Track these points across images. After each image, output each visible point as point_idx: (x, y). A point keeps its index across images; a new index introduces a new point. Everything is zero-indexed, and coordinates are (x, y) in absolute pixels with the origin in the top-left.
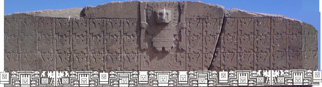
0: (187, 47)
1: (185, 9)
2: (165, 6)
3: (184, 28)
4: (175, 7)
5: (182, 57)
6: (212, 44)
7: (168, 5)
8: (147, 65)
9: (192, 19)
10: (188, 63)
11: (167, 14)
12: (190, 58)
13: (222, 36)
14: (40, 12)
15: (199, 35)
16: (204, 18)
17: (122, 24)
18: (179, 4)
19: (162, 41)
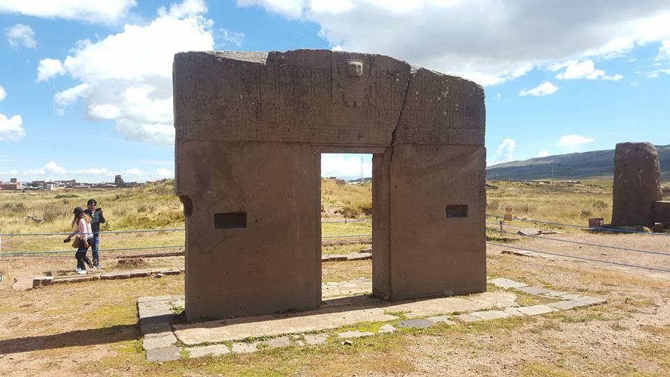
7: (360, 57)
11: (359, 66)
13: (408, 95)
14: (222, 53)
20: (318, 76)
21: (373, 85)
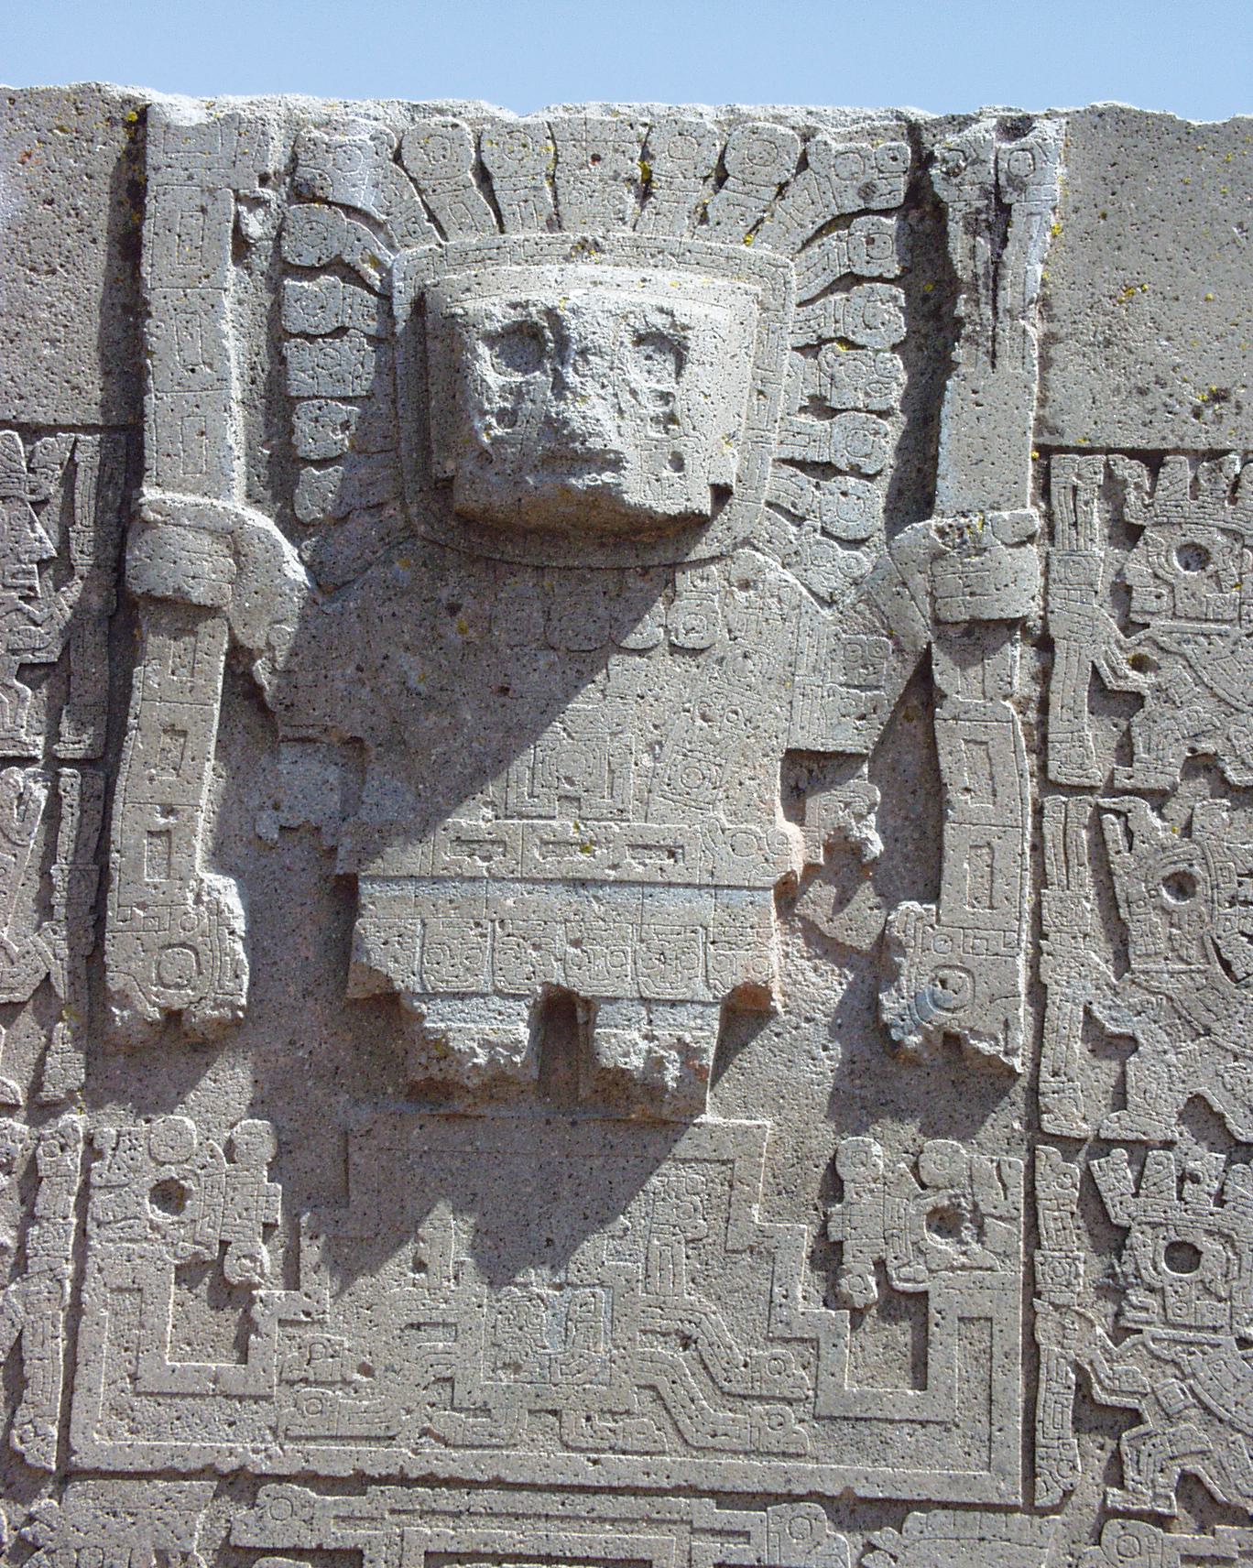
0: (1065, 1015)
2: (645, 191)
3: (1012, 624)
4: (842, 220)
5: (944, 1222)
8: (224, 1364)
9: (1179, 471)
12: (1113, 1238)
18: (923, 160)
19: (551, 865)
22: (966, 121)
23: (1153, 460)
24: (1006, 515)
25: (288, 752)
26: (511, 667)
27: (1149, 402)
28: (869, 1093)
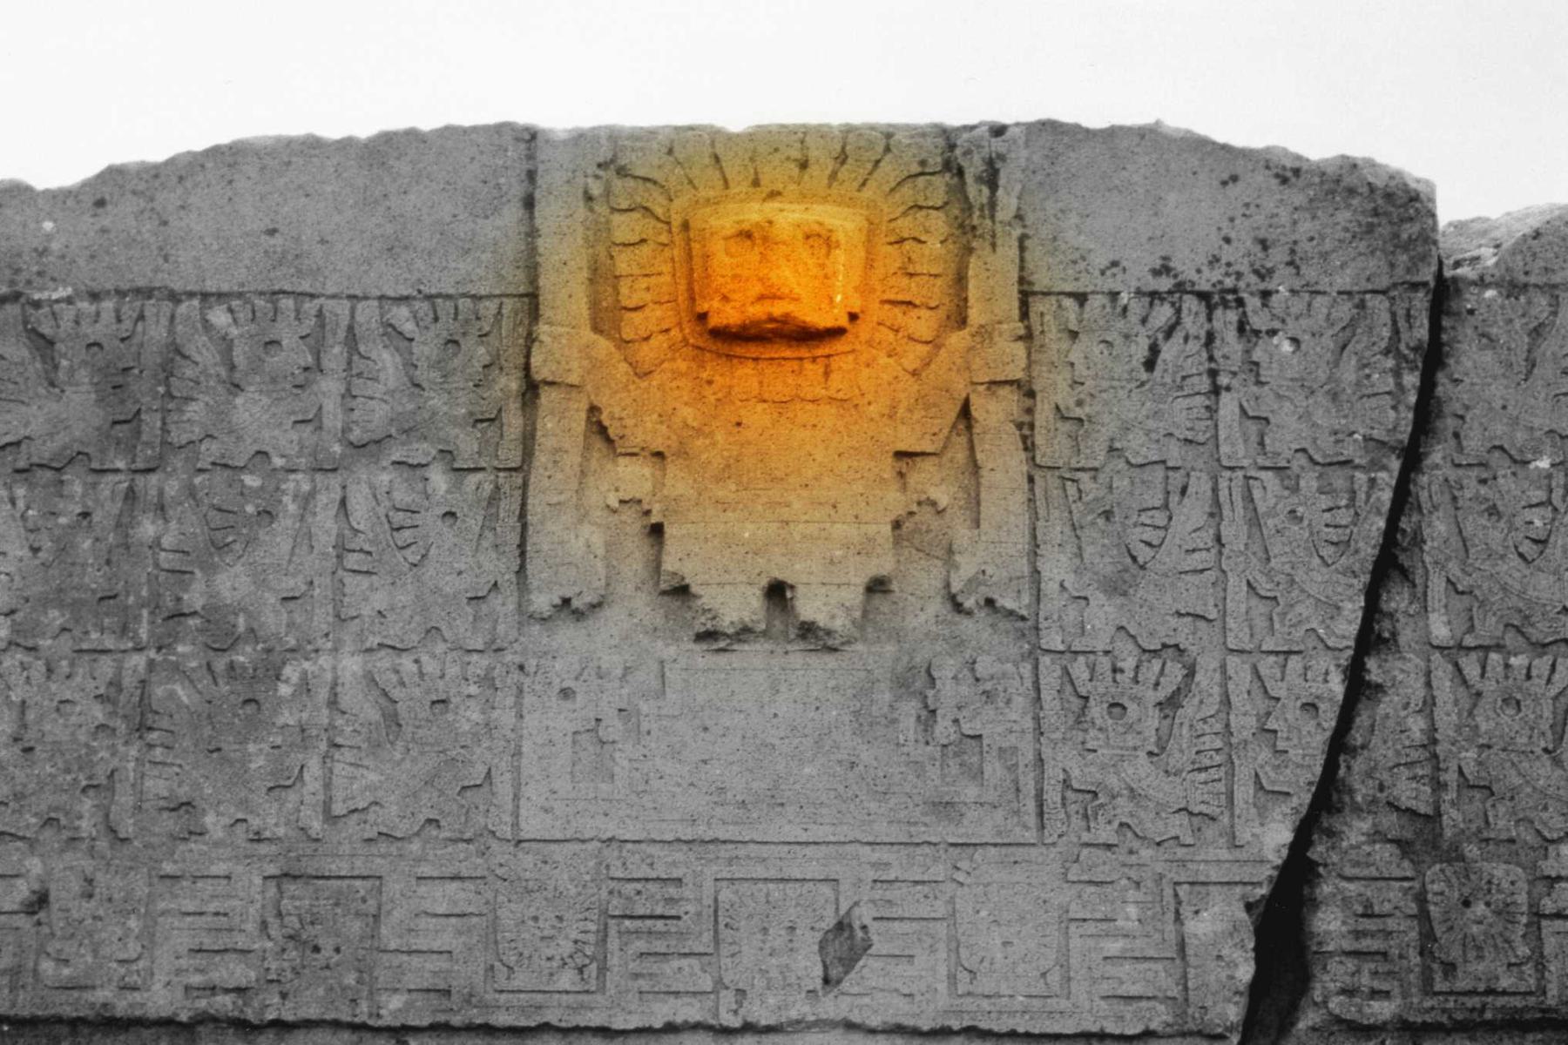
0: (1050, 587)
1: (1008, 202)
6: (1327, 552)
9: (1095, 302)
10: (1064, 760)
11: (820, 239)
13: (1428, 485)
15: (1174, 454)
16: (1229, 282)
17: (335, 355)
20: (387, 360)
21: (994, 412)
22: (973, 128)
23: (1081, 298)
24: (1005, 326)
25: (621, 460)
26: (743, 412)
27: (1077, 268)
28: (946, 632)
